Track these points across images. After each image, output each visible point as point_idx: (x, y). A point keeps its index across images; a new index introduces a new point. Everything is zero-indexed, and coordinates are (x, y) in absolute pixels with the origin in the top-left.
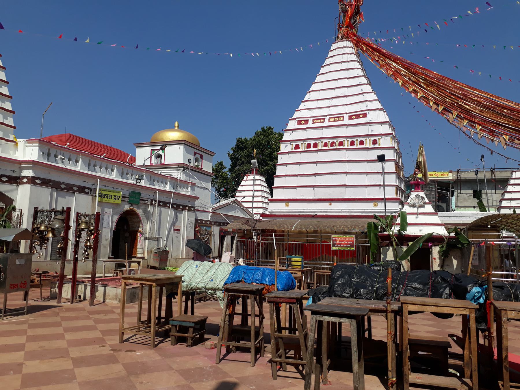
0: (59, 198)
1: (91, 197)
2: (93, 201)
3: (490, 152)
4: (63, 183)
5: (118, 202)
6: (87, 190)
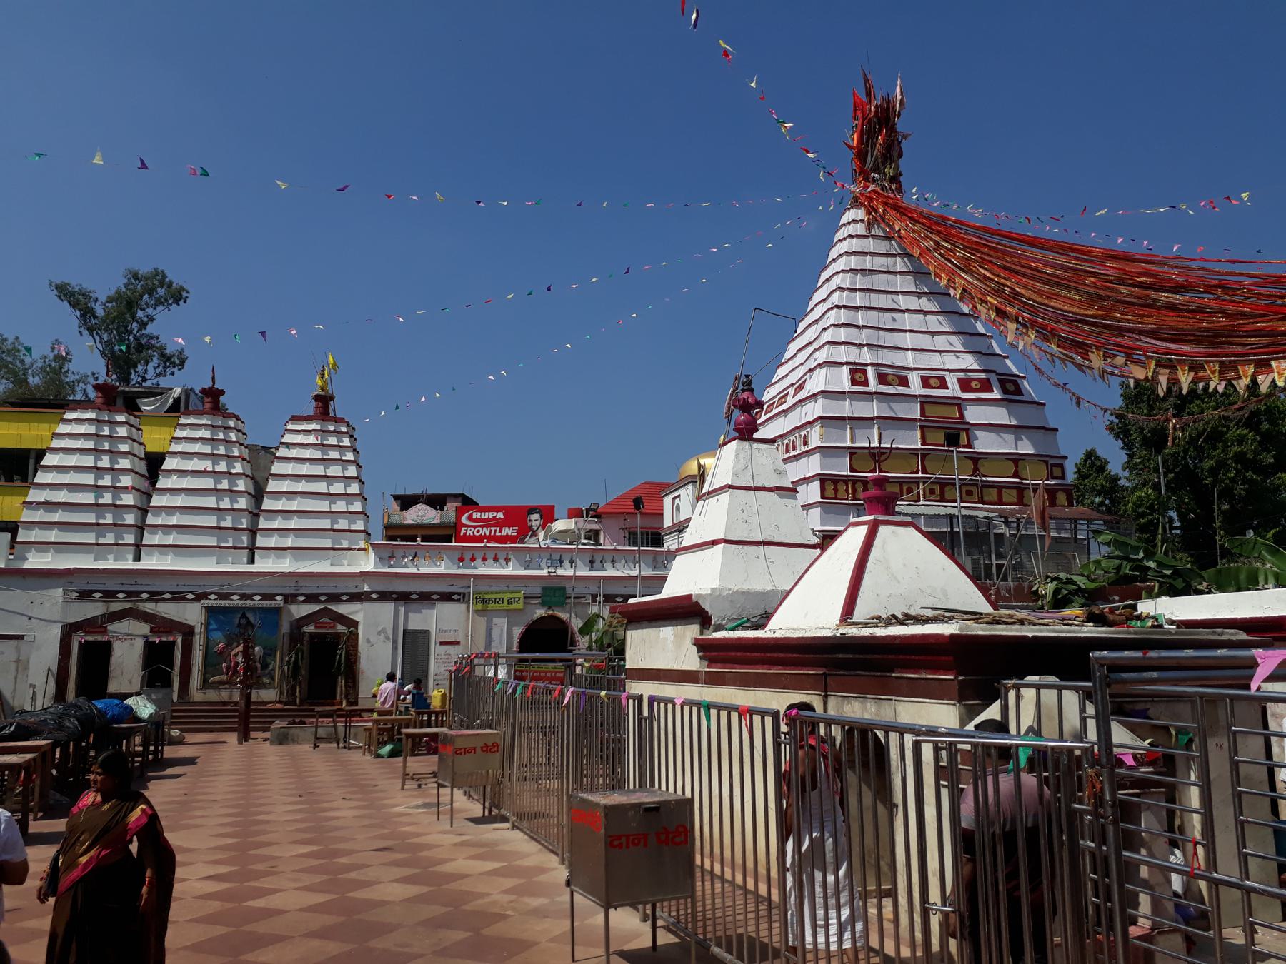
0: (411, 615)
1: (463, 606)
2: (468, 608)
3: (1074, 400)
4: (415, 593)
5: (520, 606)
6: (456, 597)
